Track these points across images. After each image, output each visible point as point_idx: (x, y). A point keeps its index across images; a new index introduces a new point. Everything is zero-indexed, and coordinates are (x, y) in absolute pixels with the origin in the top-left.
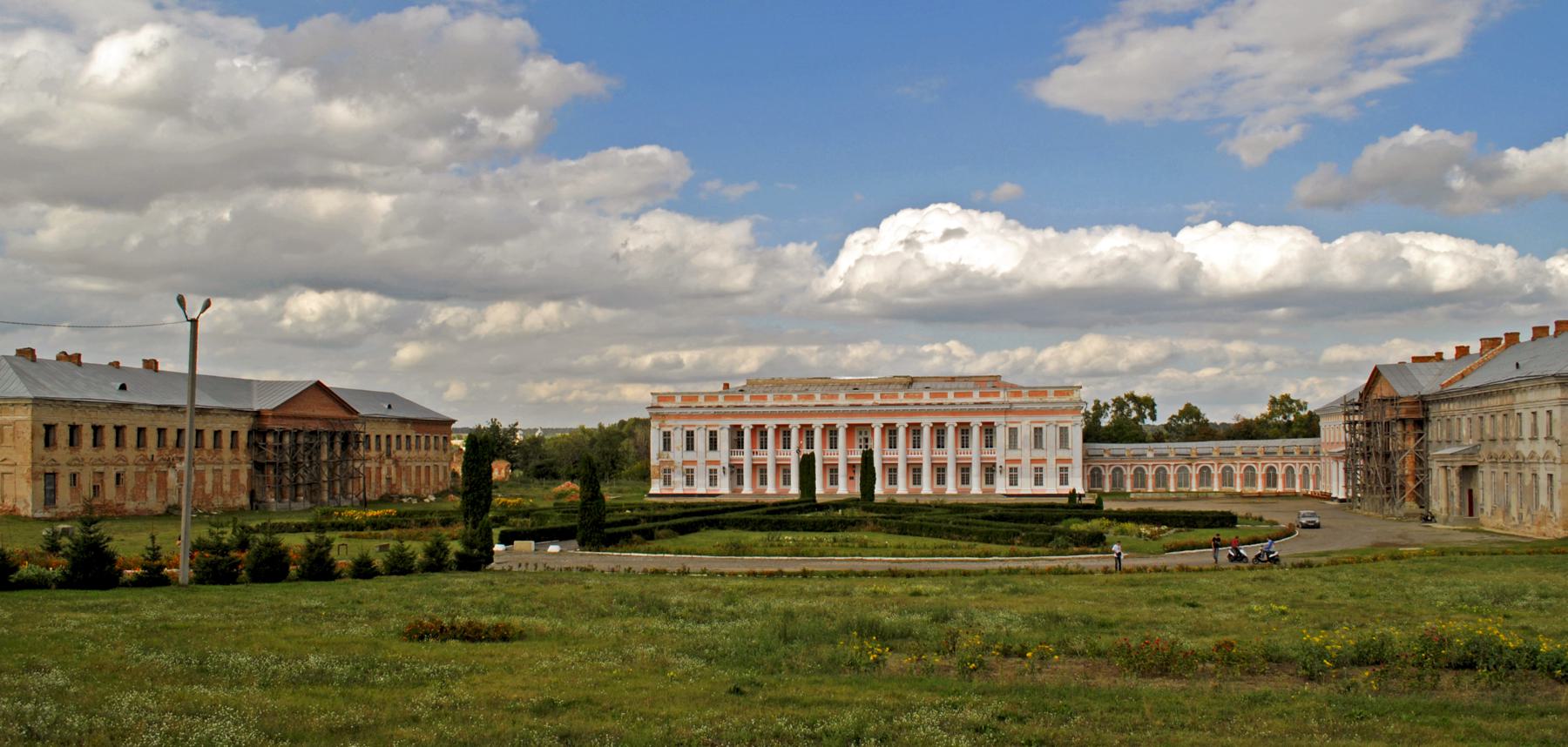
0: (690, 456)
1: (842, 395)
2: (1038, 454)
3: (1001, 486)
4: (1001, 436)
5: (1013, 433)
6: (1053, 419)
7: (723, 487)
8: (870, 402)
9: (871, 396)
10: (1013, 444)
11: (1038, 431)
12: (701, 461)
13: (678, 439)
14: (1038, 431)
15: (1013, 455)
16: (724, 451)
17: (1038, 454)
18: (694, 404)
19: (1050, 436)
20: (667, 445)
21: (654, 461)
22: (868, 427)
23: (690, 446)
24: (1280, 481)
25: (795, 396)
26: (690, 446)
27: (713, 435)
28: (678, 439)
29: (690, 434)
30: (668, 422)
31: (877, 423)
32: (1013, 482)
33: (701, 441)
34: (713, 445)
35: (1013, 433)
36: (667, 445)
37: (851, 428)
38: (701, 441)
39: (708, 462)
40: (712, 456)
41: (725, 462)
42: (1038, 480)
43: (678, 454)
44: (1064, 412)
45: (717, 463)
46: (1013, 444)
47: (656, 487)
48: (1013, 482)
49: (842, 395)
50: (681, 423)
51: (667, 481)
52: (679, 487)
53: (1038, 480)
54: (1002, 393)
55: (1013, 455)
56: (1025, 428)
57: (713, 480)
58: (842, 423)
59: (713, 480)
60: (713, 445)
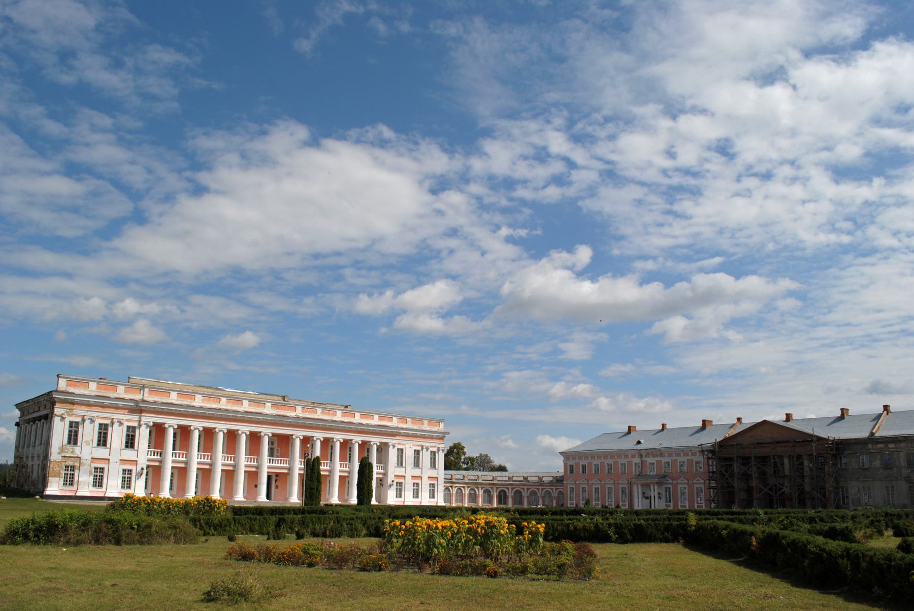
0: (102, 452)
1: (268, 405)
2: (417, 472)
5: (401, 451)
7: (139, 490)
8: (292, 414)
10: (400, 463)
11: (417, 452)
13: (89, 433)
15: (400, 471)
16: (143, 454)
17: (417, 472)
18: (112, 395)
20: (73, 438)
21: (55, 455)
23: (102, 441)
24: (510, 501)
25: (224, 400)
26: (102, 441)
28: (89, 433)
30: (80, 411)
31: (298, 434)
32: (399, 495)
33: (117, 436)
34: (130, 443)
35: (401, 451)
36: (73, 438)
38: (117, 436)
40: (129, 454)
41: (143, 462)
42: (416, 494)
43: (87, 449)
44: (432, 438)
46: (400, 463)
47: (54, 488)
48: (399, 495)
49: (268, 405)
50: (95, 413)
51: (70, 480)
52: (85, 488)
53: (416, 494)
55: (400, 471)
56: (409, 448)
57: (127, 482)
58: (267, 431)
60: (130, 443)
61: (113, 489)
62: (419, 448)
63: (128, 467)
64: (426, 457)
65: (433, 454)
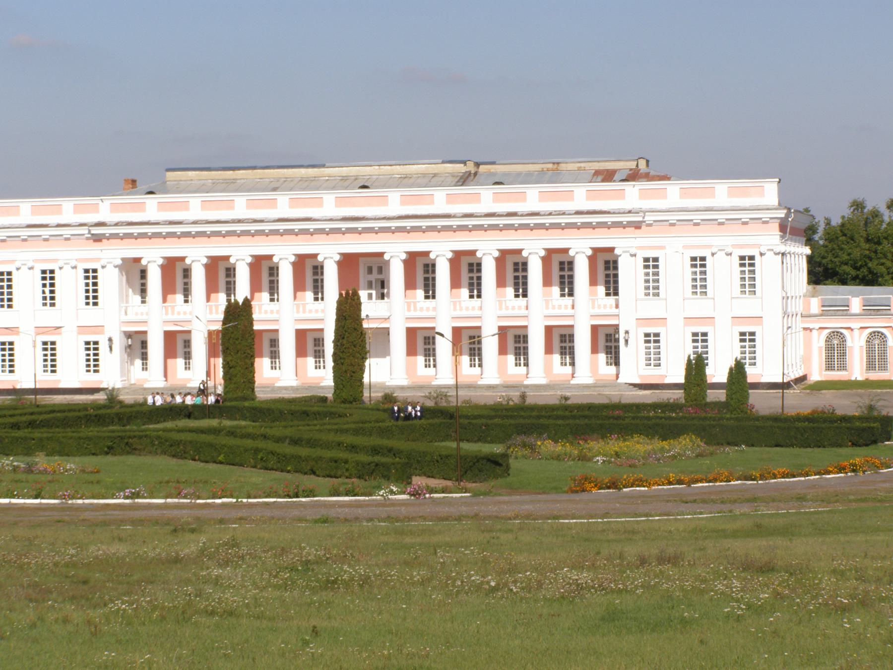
2: (699, 307)
3: (633, 368)
4: (630, 273)
9: (384, 200)
10: (652, 287)
11: (699, 262)
14: (699, 262)
17: (699, 307)
19: (723, 273)
23: (50, 300)
26: (50, 300)
27: (91, 275)
29: (48, 277)
34: (92, 297)
37: (348, 263)
39: (82, 329)
40: (91, 315)
45: (99, 329)
46: (652, 287)
55: (652, 308)
58: (329, 252)
59: (93, 363)
60: (92, 297)
61: (71, 374)
63: (92, 338)
64: (723, 273)
65: (748, 261)
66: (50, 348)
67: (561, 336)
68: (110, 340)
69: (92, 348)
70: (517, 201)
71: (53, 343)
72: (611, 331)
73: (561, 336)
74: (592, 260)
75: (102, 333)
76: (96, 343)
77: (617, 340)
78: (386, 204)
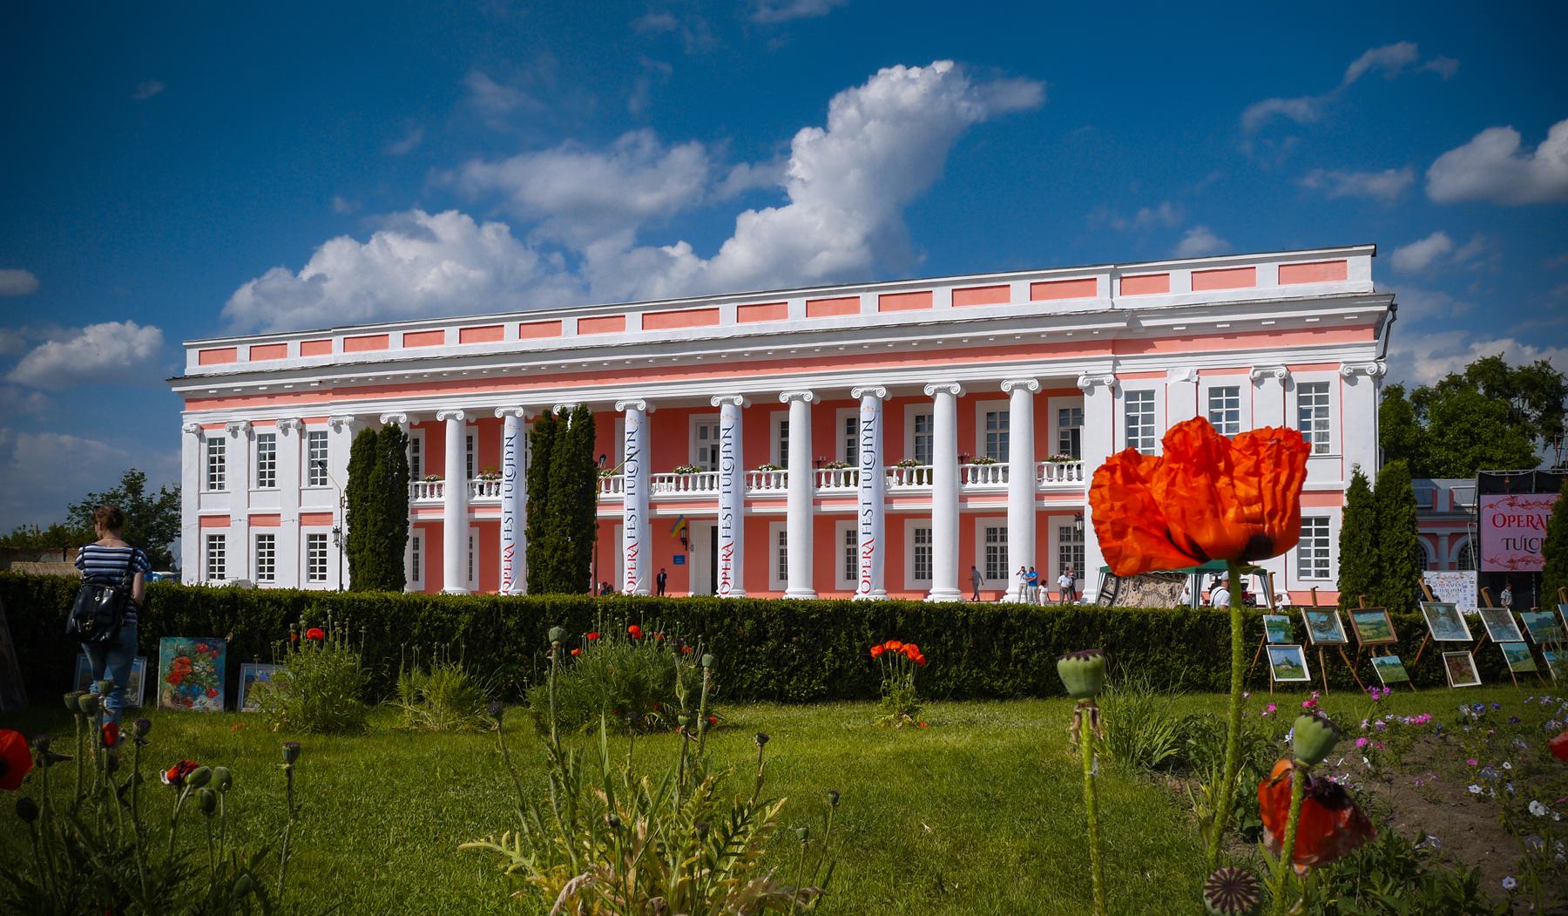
6: (1275, 357)
12: (290, 514)
22: (705, 409)
26: (266, 474)
31: (728, 392)
36: (215, 476)
54: (1103, 280)
57: (317, 567)
59: (317, 567)
60: (318, 469)
62: (1242, 381)
63: (318, 530)
66: (266, 544)
67: (989, 530)
68: (336, 531)
69: (316, 542)
70: (916, 306)
71: (271, 537)
72: (1069, 521)
73: (989, 530)
74: (1040, 402)
75: (329, 523)
76: (323, 537)
77: (1080, 535)
78: (716, 321)
